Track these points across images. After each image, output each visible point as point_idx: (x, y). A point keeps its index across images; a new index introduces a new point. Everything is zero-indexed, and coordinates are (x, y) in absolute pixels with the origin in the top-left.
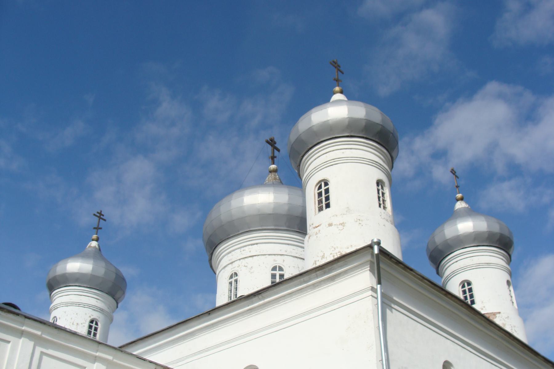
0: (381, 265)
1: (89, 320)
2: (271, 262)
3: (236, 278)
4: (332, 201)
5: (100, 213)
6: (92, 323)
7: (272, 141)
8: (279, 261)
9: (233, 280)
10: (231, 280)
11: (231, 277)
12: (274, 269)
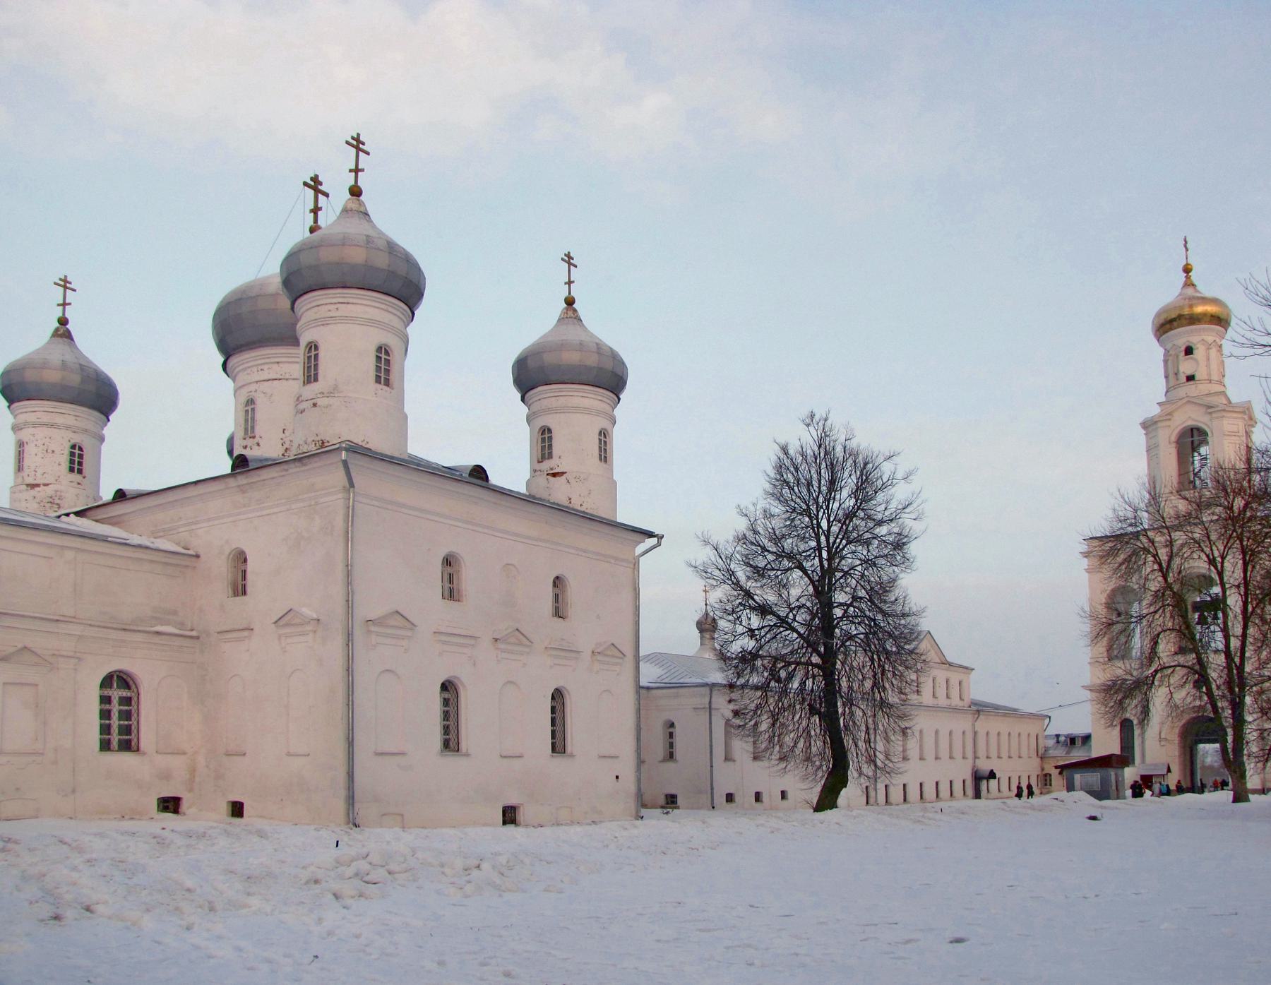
1: (69, 445)
3: (252, 407)
6: (75, 449)
9: (249, 408)
10: (246, 408)
11: (247, 405)
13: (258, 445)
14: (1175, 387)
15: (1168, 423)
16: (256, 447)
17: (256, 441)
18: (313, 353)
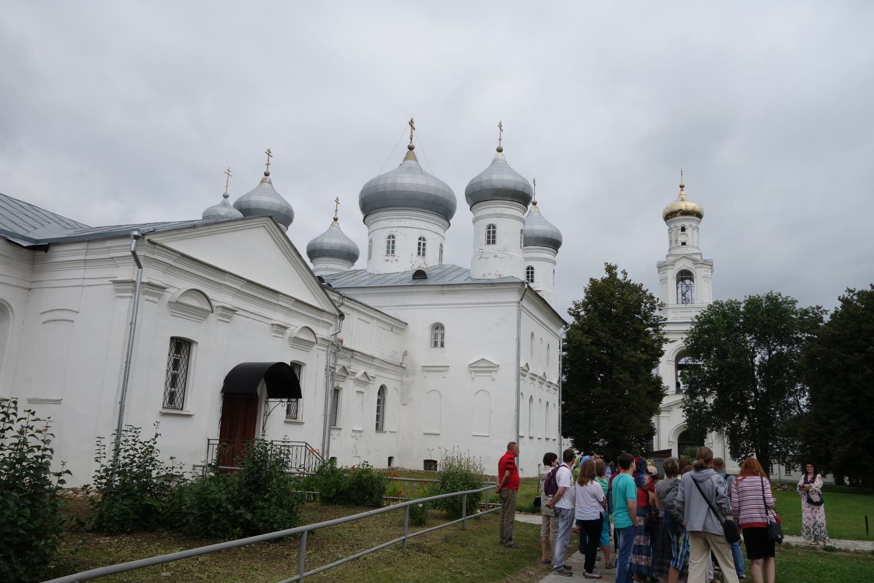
0: (526, 292)
2: (417, 234)
4: (498, 239)
5: (269, 151)
7: (412, 122)
8: (424, 234)
9: (391, 240)
10: (389, 240)
11: (389, 237)
12: (420, 239)
13: (397, 260)
14: (676, 248)
15: (672, 267)
16: (395, 262)
17: (395, 258)
18: (491, 230)
